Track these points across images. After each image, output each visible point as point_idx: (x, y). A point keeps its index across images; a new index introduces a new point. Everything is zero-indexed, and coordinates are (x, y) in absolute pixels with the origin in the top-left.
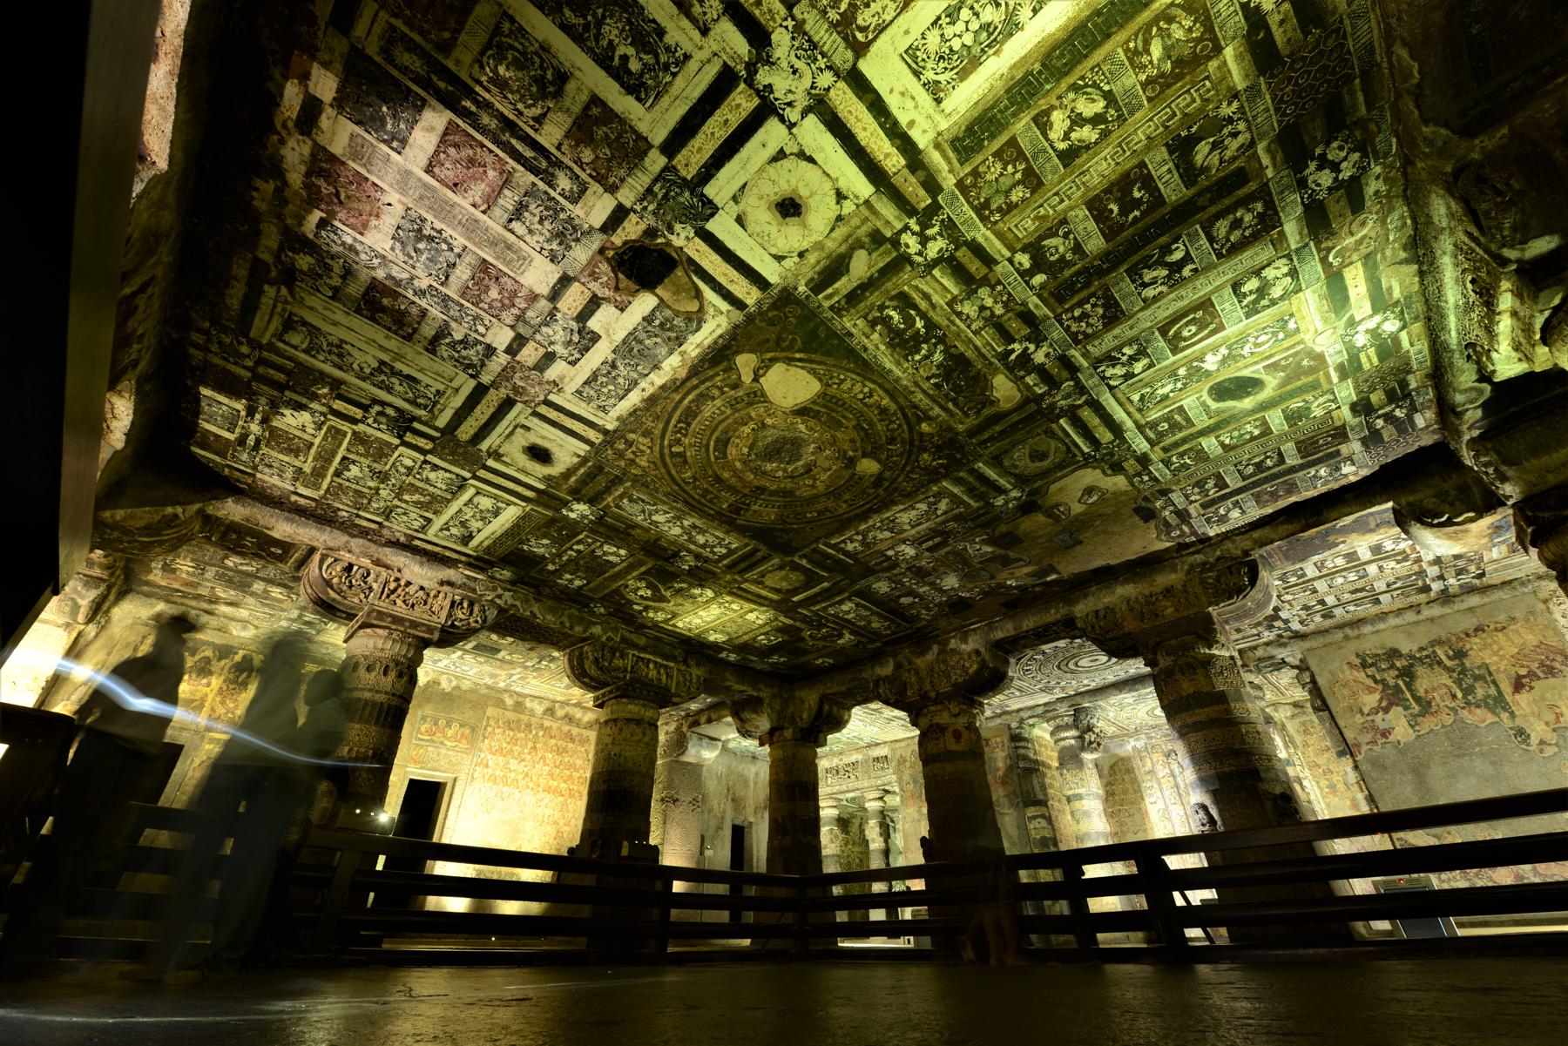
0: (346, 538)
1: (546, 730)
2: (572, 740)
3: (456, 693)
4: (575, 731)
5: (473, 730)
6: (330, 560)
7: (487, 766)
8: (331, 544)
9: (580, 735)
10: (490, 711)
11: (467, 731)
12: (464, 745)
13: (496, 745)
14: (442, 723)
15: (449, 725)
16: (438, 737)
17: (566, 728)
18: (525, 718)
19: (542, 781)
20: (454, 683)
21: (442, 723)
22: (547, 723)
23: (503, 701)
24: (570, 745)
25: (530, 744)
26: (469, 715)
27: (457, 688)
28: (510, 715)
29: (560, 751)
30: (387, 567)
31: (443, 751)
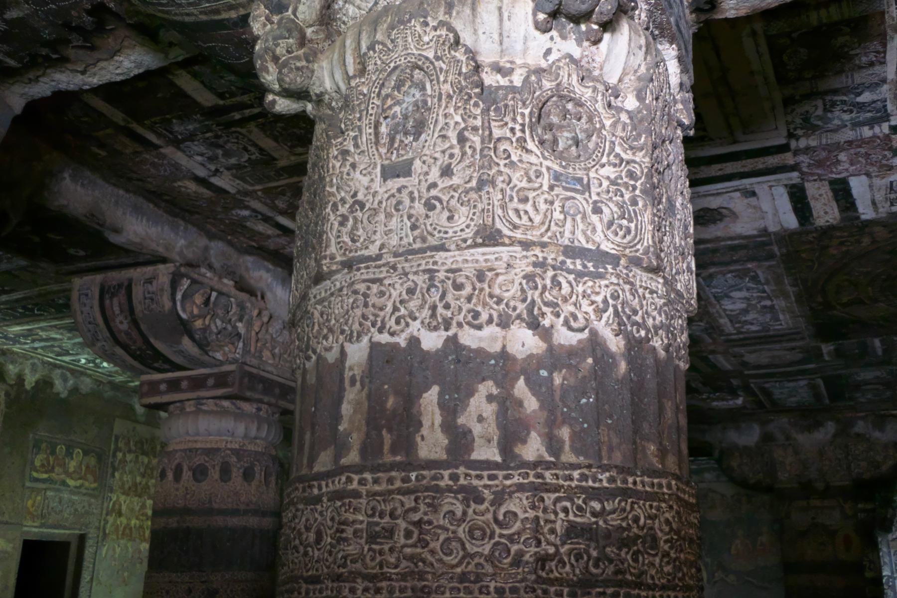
0: (203, 241)
5: (100, 458)
6: (185, 283)
7: (120, 514)
8: (189, 255)
10: (120, 427)
11: (93, 461)
14: (61, 449)
15: (69, 454)
16: (58, 474)
21: (61, 449)
23: (132, 409)
27: (75, 390)
30: (251, 292)
31: (66, 496)
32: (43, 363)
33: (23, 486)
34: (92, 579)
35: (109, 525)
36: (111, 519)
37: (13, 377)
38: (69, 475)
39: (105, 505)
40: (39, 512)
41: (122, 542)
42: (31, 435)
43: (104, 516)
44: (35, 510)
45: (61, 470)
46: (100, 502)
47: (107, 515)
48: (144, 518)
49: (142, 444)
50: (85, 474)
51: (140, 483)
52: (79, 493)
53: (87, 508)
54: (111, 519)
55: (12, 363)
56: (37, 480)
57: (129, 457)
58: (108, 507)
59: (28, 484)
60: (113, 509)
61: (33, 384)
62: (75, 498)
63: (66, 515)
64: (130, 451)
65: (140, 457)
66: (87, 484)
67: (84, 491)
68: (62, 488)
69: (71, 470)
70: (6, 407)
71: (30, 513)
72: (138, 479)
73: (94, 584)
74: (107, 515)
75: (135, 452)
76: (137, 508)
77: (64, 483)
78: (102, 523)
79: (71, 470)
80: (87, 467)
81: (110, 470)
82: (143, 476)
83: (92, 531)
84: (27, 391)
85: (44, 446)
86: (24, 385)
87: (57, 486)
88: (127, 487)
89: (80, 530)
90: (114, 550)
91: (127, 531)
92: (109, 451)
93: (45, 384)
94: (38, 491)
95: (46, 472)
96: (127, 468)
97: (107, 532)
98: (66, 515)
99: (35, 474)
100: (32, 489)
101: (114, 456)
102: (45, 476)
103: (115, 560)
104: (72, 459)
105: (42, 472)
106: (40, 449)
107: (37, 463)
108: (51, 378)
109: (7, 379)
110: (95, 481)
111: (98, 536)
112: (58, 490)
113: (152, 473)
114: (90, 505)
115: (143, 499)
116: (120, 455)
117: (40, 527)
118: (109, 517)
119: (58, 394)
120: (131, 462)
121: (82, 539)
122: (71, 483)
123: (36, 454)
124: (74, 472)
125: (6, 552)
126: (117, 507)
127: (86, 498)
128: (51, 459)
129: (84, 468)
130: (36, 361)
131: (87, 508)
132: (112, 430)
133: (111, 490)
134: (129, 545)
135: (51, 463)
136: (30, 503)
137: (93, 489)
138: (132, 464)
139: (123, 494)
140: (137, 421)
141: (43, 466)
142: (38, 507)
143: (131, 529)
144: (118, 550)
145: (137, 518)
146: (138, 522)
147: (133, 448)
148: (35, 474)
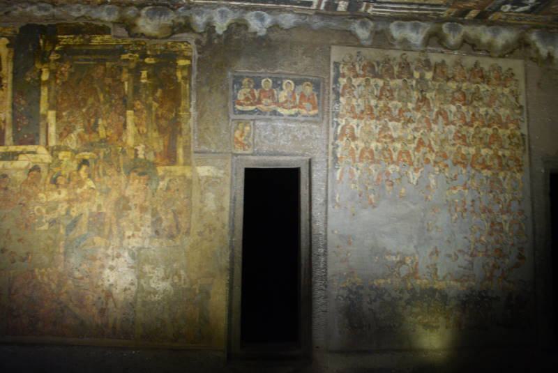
1: (438, 68)
2: (484, 78)
3: (275, 36)
4: (486, 63)
5: (317, 86)
7: (354, 138)
9: (493, 68)
10: (337, 54)
11: (308, 90)
12: (308, 110)
13: (359, 103)
15: (277, 84)
17: (470, 61)
18: (395, 54)
19: (448, 148)
20: (269, 20)
21: (266, 83)
22: (435, 58)
24: (483, 88)
25: (415, 95)
26: (303, 63)
27: (275, 27)
28: (372, 54)
29: (468, 99)
31: (280, 124)
32: (233, 8)
33: (229, 117)
34: (326, 201)
35: (340, 149)
36: (341, 143)
37: (202, 26)
38: (282, 105)
39: (332, 130)
40: (251, 141)
41: (361, 165)
42: (230, 73)
43: (331, 139)
44: (245, 139)
45: (269, 101)
46: (324, 127)
47: (335, 139)
48: (388, 140)
49: (373, 67)
50: (300, 103)
51: (376, 106)
52: (296, 121)
53: (308, 134)
54: (341, 143)
55: (198, 14)
56: (243, 112)
57: (355, 82)
58: (336, 132)
59: (232, 116)
60: (343, 133)
61: (225, 29)
62: (293, 125)
63: (282, 142)
64: (357, 76)
65: (372, 81)
66: (304, 112)
67: (303, 119)
68: (274, 117)
69: (282, 99)
70: (199, 53)
71: (238, 142)
72: (373, 102)
73: (330, 206)
74: (335, 139)
75: (364, 76)
76: (377, 131)
77: (275, 113)
78: (331, 147)
79: (282, 99)
80: (302, 96)
81: (332, 96)
82: (379, 98)
83: (317, 155)
84: (219, 36)
85: (245, 81)
86: (215, 31)
87: (267, 116)
88: (358, 111)
89: (303, 155)
90: (351, 173)
91: (367, 154)
92: (329, 78)
93: (241, 25)
94: (246, 123)
95: (252, 104)
96: (355, 92)
97: (339, 156)
98: (282, 142)
99: (239, 108)
100: (239, 121)
101: (336, 81)
102: (251, 108)
103: (354, 182)
104: (282, 89)
105: (248, 105)
106: (241, 84)
107: (241, 97)
108: (244, 20)
109: (194, 27)
110: (314, 108)
111: (327, 160)
112: (270, 119)
113: (392, 95)
114: (311, 131)
115: (383, 122)
116: (343, 81)
117: (252, 155)
118: (338, 142)
119: (255, 33)
120: (359, 86)
121: (310, 162)
122: (285, 112)
123: (238, 90)
124: (286, 101)
125: (217, 178)
126: (348, 131)
127: (305, 125)
128: (256, 93)
129: (298, 97)
130: (224, 8)
131: (308, 134)
132: (329, 59)
133: (337, 115)
134: (372, 167)
135: (257, 95)
136: (237, 134)
137: (314, 116)
138: (362, 88)
139: (354, 118)
140: (362, 46)
141: (247, 99)
142: (248, 137)
143: (371, 152)
144: (357, 174)
145: (378, 141)
146: (379, 144)
147: (362, 72)
148: (239, 108)
